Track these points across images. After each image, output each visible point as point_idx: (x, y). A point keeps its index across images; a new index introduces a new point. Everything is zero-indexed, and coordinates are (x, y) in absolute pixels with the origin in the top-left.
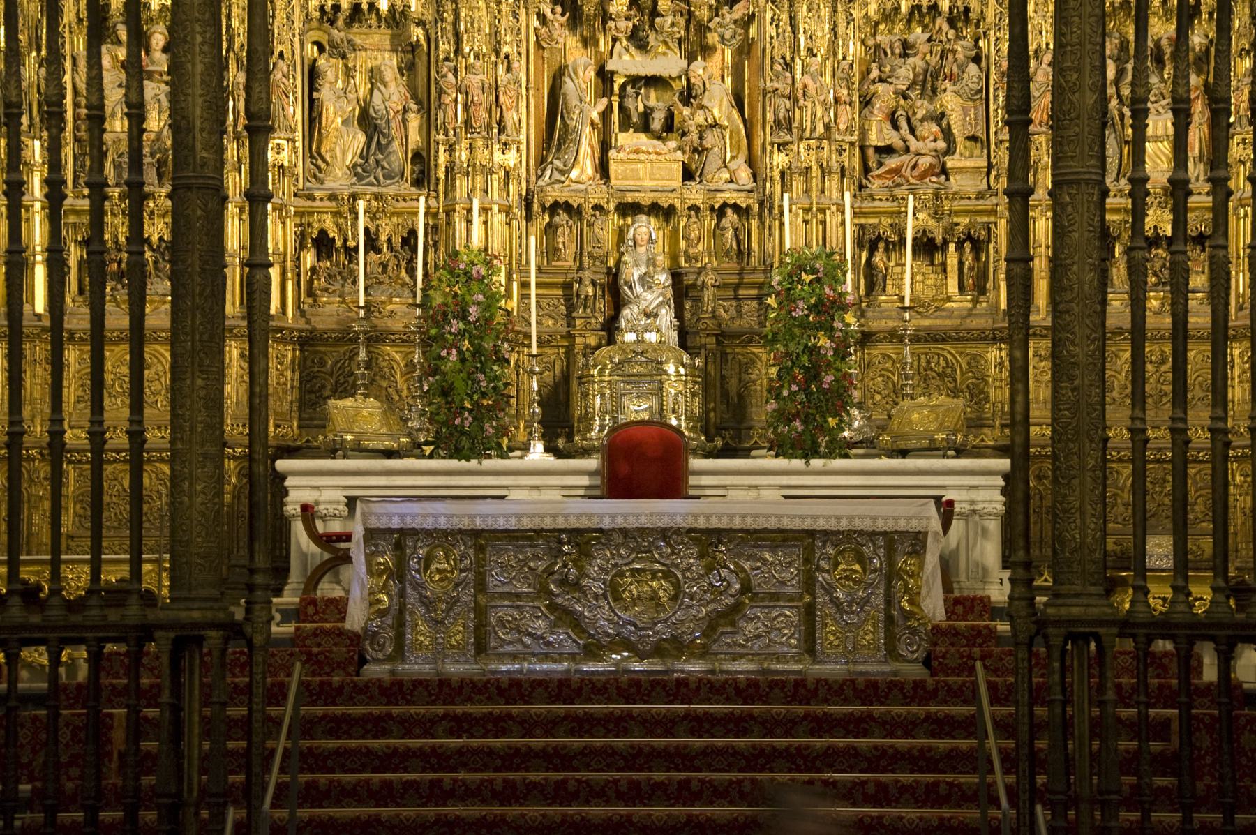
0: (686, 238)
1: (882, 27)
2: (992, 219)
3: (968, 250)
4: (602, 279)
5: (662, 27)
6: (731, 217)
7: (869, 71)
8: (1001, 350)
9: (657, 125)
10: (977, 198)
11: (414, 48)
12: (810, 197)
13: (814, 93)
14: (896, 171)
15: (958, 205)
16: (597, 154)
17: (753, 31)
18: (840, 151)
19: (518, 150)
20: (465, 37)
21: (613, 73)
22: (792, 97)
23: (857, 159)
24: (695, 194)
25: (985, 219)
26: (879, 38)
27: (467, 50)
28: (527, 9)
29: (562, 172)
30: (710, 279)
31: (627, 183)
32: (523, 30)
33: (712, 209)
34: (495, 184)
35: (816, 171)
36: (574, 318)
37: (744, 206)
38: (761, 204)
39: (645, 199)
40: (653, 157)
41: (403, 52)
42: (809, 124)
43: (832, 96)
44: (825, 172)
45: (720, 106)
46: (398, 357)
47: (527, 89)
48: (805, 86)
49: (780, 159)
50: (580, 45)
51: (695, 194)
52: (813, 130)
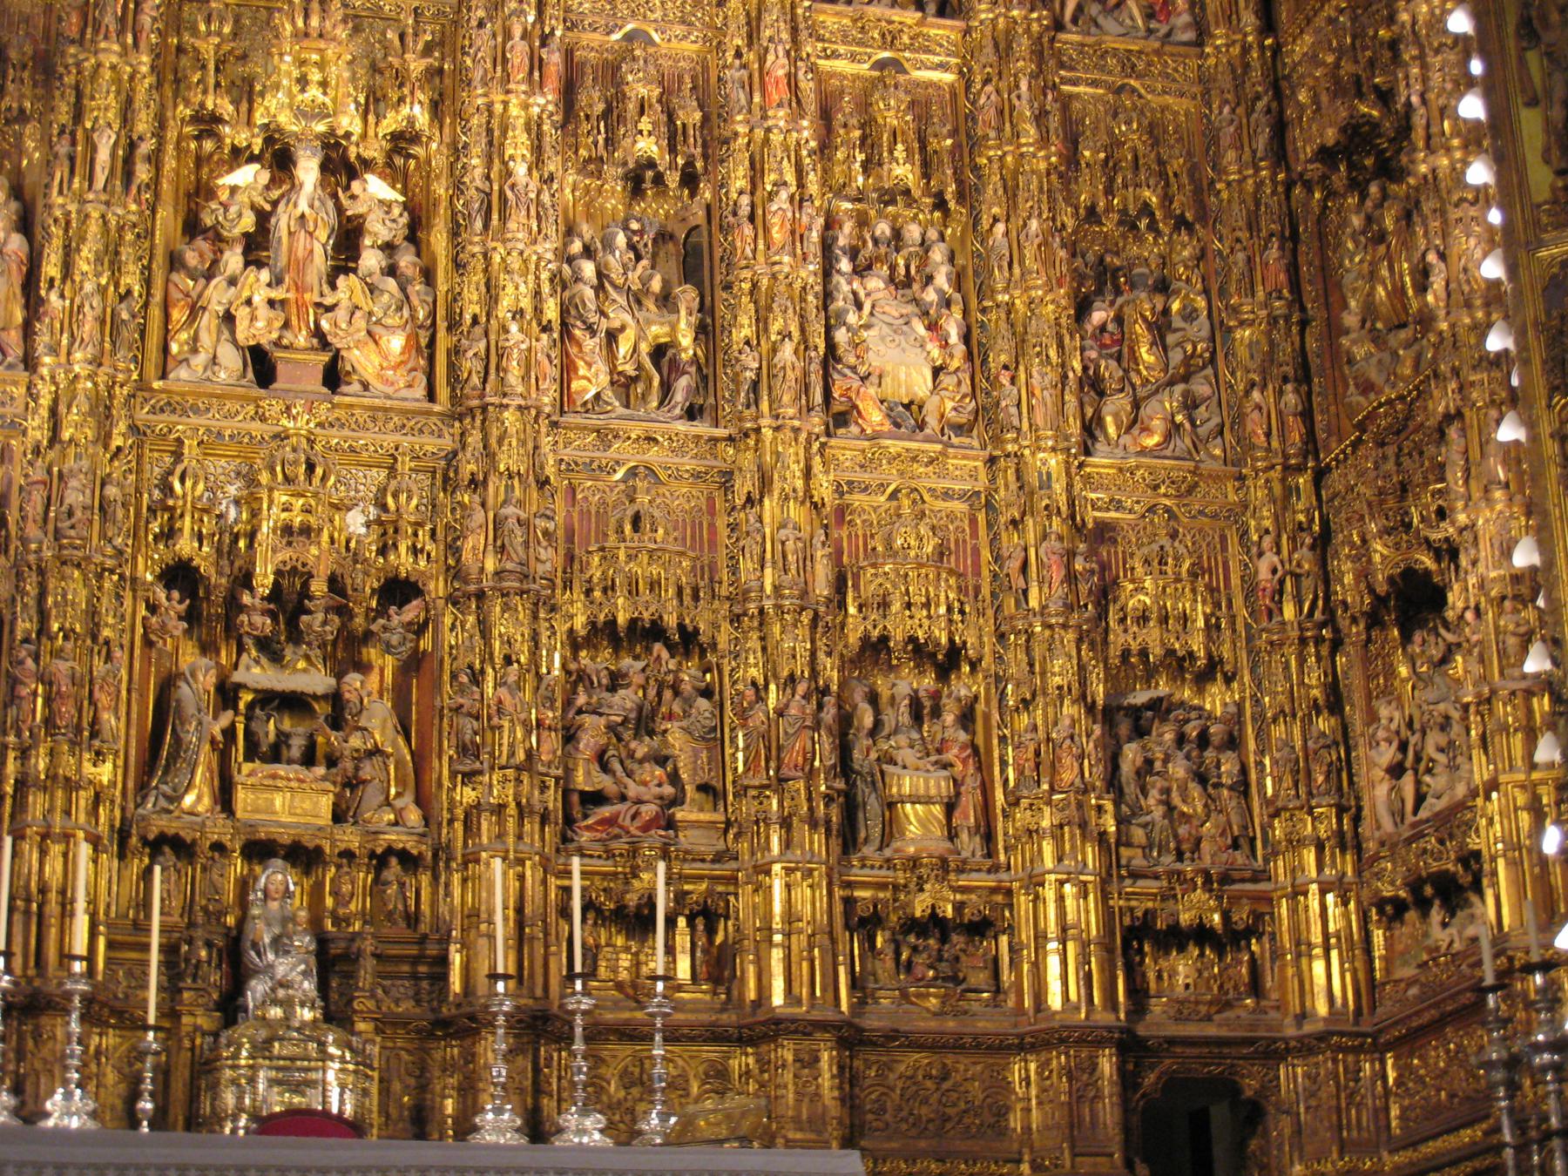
0: (335, 893)
1: (583, 653)
2: (731, 889)
3: (701, 927)
5: (309, 626)
6: (394, 868)
10: (713, 861)
12: (504, 843)
13: (511, 709)
14: (611, 821)
17: (426, 643)
18: (544, 788)
19: (115, 766)
20: (54, 612)
21: (239, 686)
23: (560, 805)
25: (720, 888)
27: (55, 627)
28: (134, 591)
29: (170, 799)
30: (368, 946)
31: (258, 816)
32: (128, 617)
34: (82, 803)
35: (512, 810)
36: (180, 991)
37: (415, 852)
38: (435, 855)
39: (286, 840)
40: (294, 784)
42: (505, 749)
43: (533, 717)
45: (383, 728)
47: (129, 691)
48: (500, 702)
49: (467, 795)
50: (197, 651)
51: (350, 837)
52: (512, 754)
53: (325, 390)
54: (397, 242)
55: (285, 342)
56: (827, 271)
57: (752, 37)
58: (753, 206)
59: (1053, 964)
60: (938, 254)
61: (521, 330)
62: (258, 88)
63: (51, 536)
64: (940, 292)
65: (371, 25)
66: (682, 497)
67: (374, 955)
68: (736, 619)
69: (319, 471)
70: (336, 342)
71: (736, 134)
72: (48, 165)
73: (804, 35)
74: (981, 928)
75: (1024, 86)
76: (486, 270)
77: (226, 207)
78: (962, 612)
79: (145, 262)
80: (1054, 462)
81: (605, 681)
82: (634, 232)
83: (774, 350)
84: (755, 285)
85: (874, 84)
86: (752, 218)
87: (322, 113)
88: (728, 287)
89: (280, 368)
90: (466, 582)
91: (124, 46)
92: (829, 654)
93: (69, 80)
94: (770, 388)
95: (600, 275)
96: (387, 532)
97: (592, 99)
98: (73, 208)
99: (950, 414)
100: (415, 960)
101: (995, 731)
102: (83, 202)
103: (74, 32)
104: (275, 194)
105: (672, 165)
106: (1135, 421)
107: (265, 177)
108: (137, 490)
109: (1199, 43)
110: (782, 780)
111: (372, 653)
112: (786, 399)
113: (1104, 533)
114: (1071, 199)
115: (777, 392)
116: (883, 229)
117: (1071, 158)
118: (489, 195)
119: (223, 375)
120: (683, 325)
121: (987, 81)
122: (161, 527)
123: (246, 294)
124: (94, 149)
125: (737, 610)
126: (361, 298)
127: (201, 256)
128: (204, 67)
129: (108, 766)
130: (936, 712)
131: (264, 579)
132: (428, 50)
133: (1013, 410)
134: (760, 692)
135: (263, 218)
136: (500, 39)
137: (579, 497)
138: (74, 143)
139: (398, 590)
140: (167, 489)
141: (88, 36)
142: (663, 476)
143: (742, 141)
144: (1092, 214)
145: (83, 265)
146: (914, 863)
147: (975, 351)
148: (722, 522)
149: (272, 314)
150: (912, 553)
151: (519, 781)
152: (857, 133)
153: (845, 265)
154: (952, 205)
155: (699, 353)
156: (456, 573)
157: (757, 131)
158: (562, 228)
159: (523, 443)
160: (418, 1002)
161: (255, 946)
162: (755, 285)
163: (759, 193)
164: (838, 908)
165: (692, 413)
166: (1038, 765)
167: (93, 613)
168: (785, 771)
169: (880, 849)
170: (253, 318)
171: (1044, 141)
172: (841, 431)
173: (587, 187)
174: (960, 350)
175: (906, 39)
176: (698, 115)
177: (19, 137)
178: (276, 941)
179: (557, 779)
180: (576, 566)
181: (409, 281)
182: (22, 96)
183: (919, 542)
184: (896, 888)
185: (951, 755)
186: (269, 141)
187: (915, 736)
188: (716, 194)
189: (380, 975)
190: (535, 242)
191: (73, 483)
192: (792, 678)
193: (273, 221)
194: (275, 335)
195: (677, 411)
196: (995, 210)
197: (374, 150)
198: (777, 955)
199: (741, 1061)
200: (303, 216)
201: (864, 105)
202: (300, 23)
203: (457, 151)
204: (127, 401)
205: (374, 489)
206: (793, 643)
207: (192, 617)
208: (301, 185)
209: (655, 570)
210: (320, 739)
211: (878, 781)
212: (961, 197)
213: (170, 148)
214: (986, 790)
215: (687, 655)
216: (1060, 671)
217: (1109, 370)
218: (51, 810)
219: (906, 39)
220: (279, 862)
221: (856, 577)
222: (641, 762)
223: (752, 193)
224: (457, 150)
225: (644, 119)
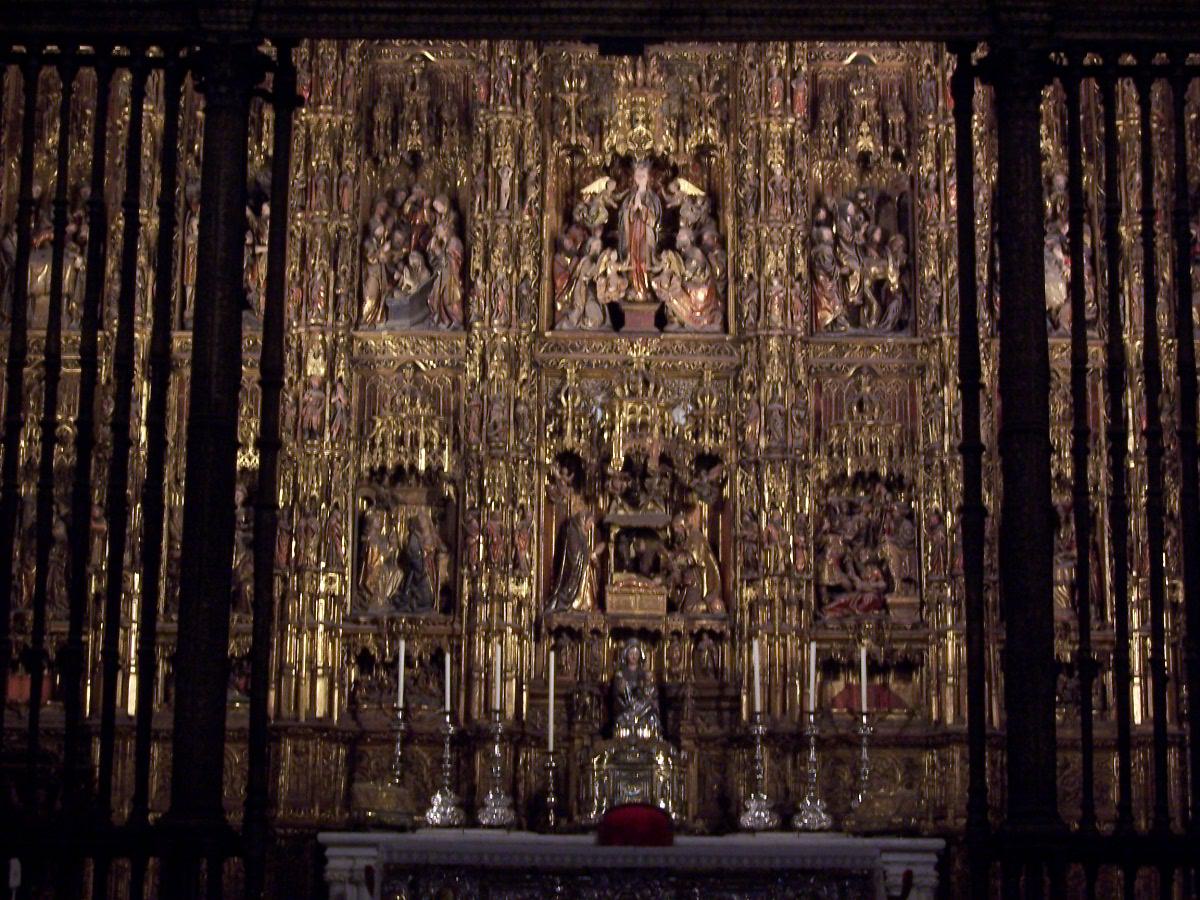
1: (832, 491)
4: (597, 691)
5: (651, 485)
6: (707, 641)
7: (822, 524)
8: (933, 755)
11: (446, 501)
14: (845, 605)
15: (895, 635)
17: (726, 491)
18: (799, 587)
19: (530, 584)
21: (609, 524)
24: (678, 623)
25: (919, 646)
26: (829, 499)
28: (539, 469)
30: (689, 692)
33: (691, 634)
34: (510, 610)
36: (573, 724)
37: (718, 631)
39: (635, 624)
41: (437, 505)
44: (786, 603)
46: (425, 755)
49: (748, 593)
51: (678, 623)
52: (776, 568)
53: (656, 330)
55: (630, 298)
58: (938, 180)
59: (1136, 692)
61: (781, 282)
62: (606, 124)
63: (484, 440)
65: (680, 70)
66: (892, 387)
67: (693, 698)
68: (928, 467)
69: (652, 386)
70: (663, 296)
71: (928, 129)
72: (473, 188)
76: (758, 240)
77: (589, 207)
79: (537, 251)
81: (845, 510)
82: (862, 201)
84: (939, 237)
86: (937, 189)
87: (647, 139)
88: (923, 237)
89: (628, 317)
90: (748, 453)
91: (515, 107)
94: (948, 309)
95: (837, 237)
97: (829, 112)
98: (488, 223)
100: (719, 699)
102: (495, 218)
103: (482, 98)
104: (620, 196)
107: (613, 186)
111: (693, 497)
118: (759, 190)
119: (590, 324)
120: (891, 269)
122: (554, 427)
123: (602, 270)
124: (500, 181)
125: (929, 462)
126: (675, 267)
127: (575, 241)
128: (568, 113)
129: (526, 584)
131: (618, 457)
132: (718, 86)
134: (942, 520)
135: (614, 215)
136: (763, 77)
137: (824, 390)
138: (487, 176)
139: (707, 461)
141: (492, 101)
142: (879, 371)
143: (931, 133)
147: (1098, 267)
148: (920, 401)
149: (619, 281)
151: (782, 584)
155: (906, 284)
157: (940, 126)
158: (812, 199)
159: (782, 360)
160: (720, 723)
161: (622, 696)
162: (939, 237)
163: (942, 173)
165: (900, 326)
167: (512, 487)
170: (607, 286)
173: (832, 167)
176: (902, 117)
178: (634, 692)
179: (809, 582)
180: (822, 436)
181: (712, 249)
182: (452, 145)
189: (698, 708)
190: (789, 221)
193: (620, 214)
194: (622, 295)
195: (889, 327)
198: (949, 693)
199: (928, 758)
200: (638, 210)
202: (630, 77)
203: (738, 155)
204: (530, 345)
205: (690, 392)
207: (578, 484)
208: (638, 188)
213: (551, 170)
218: (491, 615)
220: (635, 641)
223: (938, 169)
224: (738, 154)
225: (864, 124)
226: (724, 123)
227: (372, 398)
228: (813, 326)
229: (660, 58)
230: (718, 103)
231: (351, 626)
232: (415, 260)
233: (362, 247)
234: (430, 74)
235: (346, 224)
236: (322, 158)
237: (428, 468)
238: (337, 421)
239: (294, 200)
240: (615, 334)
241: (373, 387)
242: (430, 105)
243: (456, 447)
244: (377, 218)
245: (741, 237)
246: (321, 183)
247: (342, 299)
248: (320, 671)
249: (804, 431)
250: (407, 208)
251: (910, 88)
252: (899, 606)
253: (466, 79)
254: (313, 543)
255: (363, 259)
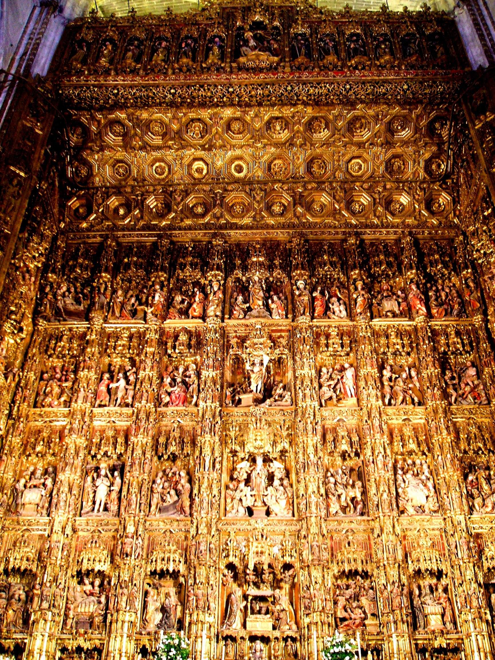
0: (274, 649)
6: (289, 642)
9: (263, 611)
11: (181, 585)
15: (370, 638)
16: (242, 621)
17: (296, 580)
18: (328, 617)
21: (248, 595)
22: (310, 599)
24: (277, 634)
25: (380, 642)
35: (320, 623)
38: (300, 637)
39: (259, 634)
44: (323, 624)
49: (307, 620)
51: (277, 634)
52: (318, 608)
54: (283, 477)
56: (395, 474)
57: (369, 417)
60: (425, 467)
64: (427, 477)
66: (361, 537)
68: (378, 567)
69: (265, 537)
72: (195, 466)
73: (383, 415)
74: (456, 650)
75: (442, 420)
77: (239, 473)
78: (440, 561)
80: (462, 518)
81: (345, 587)
83: (382, 495)
85: (403, 425)
86: (373, 462)
87: (261, 448)
88: (369, 481)
90: (304, 563)
92: (404, 575)
93: (199, 445)
96: (283, 551)
97: (330, 437)
98: (200, 476)
99: (432, 508)
101: (454, 594)
102: (203, 474)
103: (199, 433)
105: (352, 451)
106: (484, 505)
107: (248, 464)
108: (219, 545)
109: (489, 403)
110: (393, 611)
111: (282, 584)
112: (386, 508)
113: (478, 536)
114: (459, 448)
115: (383, 506)
116: (410, 462)
117: (458, 438)
121: (432, 420)
126: (273, 492)
127: (234, 486)
130: (437, 589)
131: (251, 566)
132: (288, 429)
133: (449, 505)
135: (249, 476)
139: (287, 567)
140: (227, 544)
142: (355, 531)
143: (369, 443)
144: (465, 452)
145: (202, 490)
146: (433, 632)
148: (372, 542)
150: (425, 546)
151: (321, 615)
152: (400, 438)
153: (400, 472)
154: (427, 453)
156: (302, 561)
158: (325, 470)
159: (317, 526)
164: (413, 646)
165: (362, 514)
166: (466, 602)
167: (208, 578)
168: (394, 608)
169: (424, 628)
171: (449, 434)
172: (402, 515)
174: (432, 490)
175: (410, 413)
176: (357, 438)
177: (189, 460)
181: (287, 487)
183: (426, 543)
184: (429, 639)
185: (442, 601)
186: (250, 456)
187: (431, 596)
188: (364, 457)
191: (202, 544)
192: (393, 583)
196: (438, 453)
197: (276, 455)
201: (401, 430)
203: (296, 453)
206: (393, 573)
207: (235, 578)
209: (355, 556)
210: (270, 608)
211: (422, 609)
212: (429, 451)
214: (453, 610)
215: (367, 579)
216: (469, 575)
217: (475, 492)
219: (410, 413)
220: (258, 642)
221: (410, 554)
222: (355, 608)
226: (290, 443)
227: (153, 543)
228: (328, 514)
229: (266, 420)
230: (289, 435)
231: (139, 636)
232: (173, 492)
233: (152, 487)
234: (181, 427)
235: (146, 478)
236: (138, 452)
237: (174, 570)
238: (138, 551)
239: (127, 468)
240: (249, 518)
241: (153, 539)
242: (180, 437)
243: (186, 562)
244: (158, 478)
245: (298, 482)
246: (137, 462)
247: (143, 505)
248: (123, 654)
249: (327, 554)
250: (170, 475)
251: (359, 429)
252: (370, 625)
253: (194, 428)
254: (125, 599)
255: (152, 491)
